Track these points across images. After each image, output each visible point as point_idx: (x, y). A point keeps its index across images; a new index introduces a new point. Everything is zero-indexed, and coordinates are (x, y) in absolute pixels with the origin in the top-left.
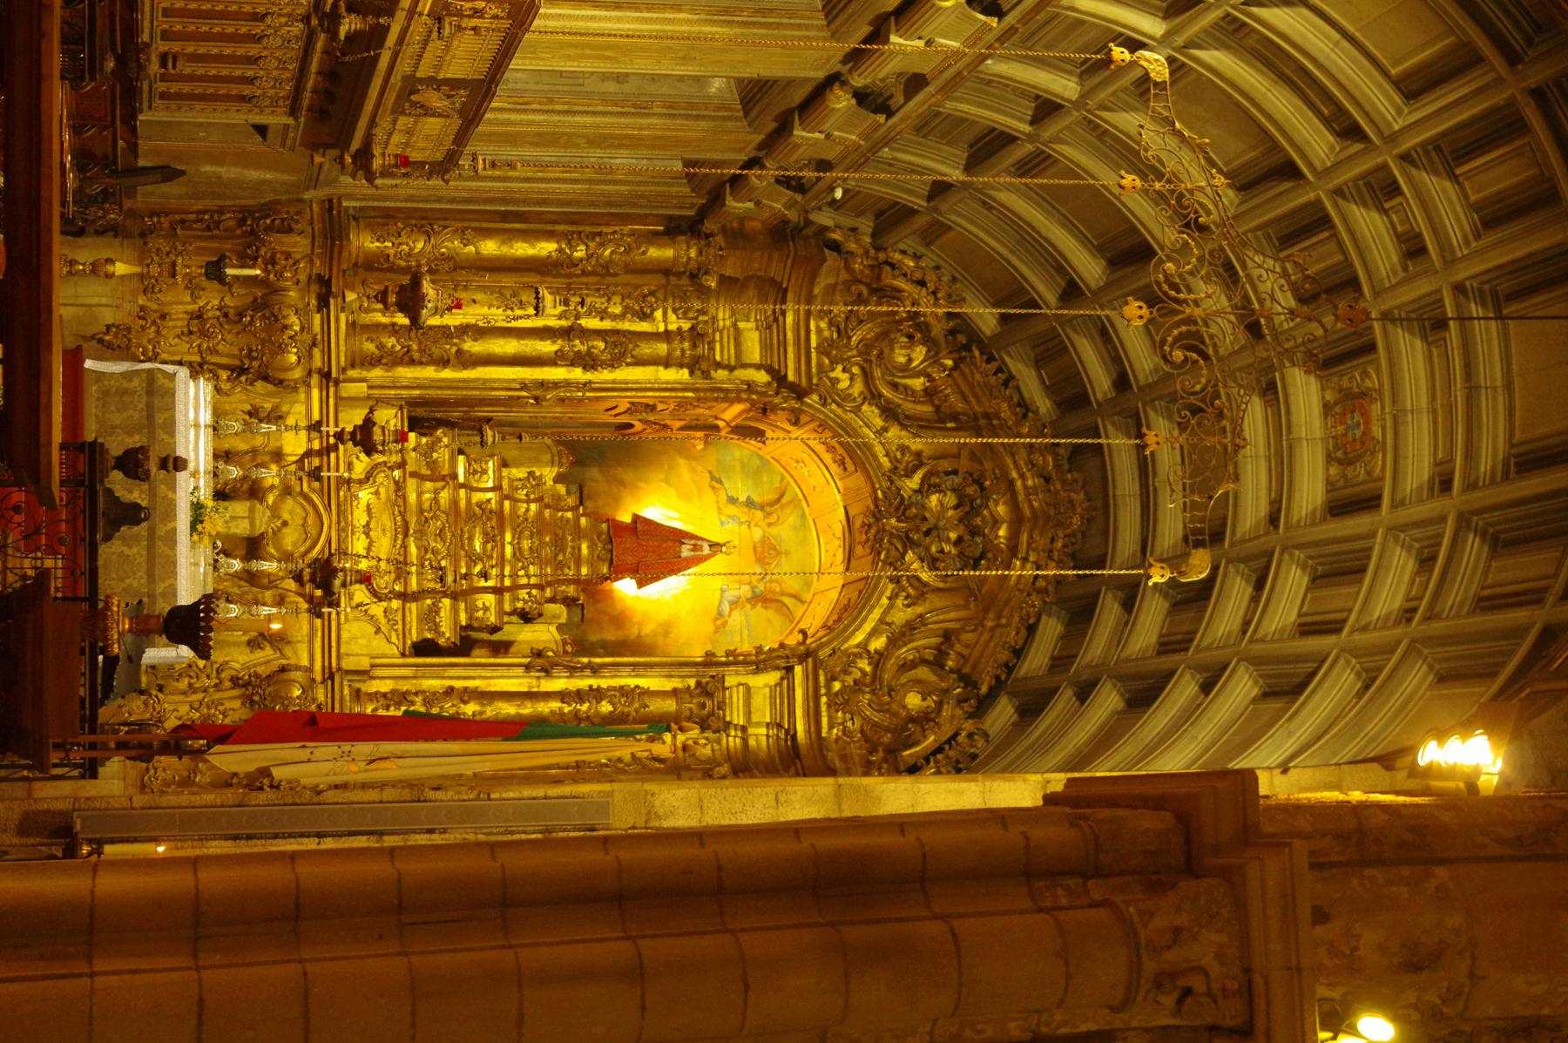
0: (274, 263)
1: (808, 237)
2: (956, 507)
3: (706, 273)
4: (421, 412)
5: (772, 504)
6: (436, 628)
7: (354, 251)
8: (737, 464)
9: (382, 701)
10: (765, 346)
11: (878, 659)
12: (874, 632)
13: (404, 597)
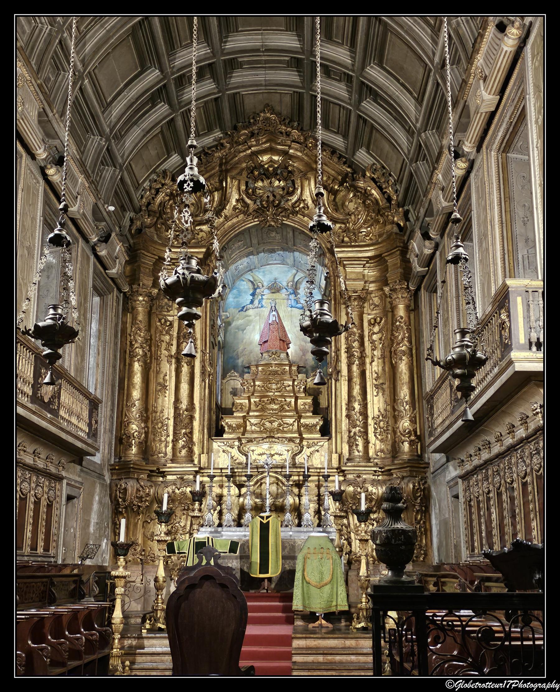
0: (142, 497)
1: (134, 243)
2: (263, 181)
3: (151, 293)
4: (213, 431)
5: (254, 285)
6: (315, 425)
7: (136, 459)
8: (236, 300)
9: (354, 447)
13: (302, 439)
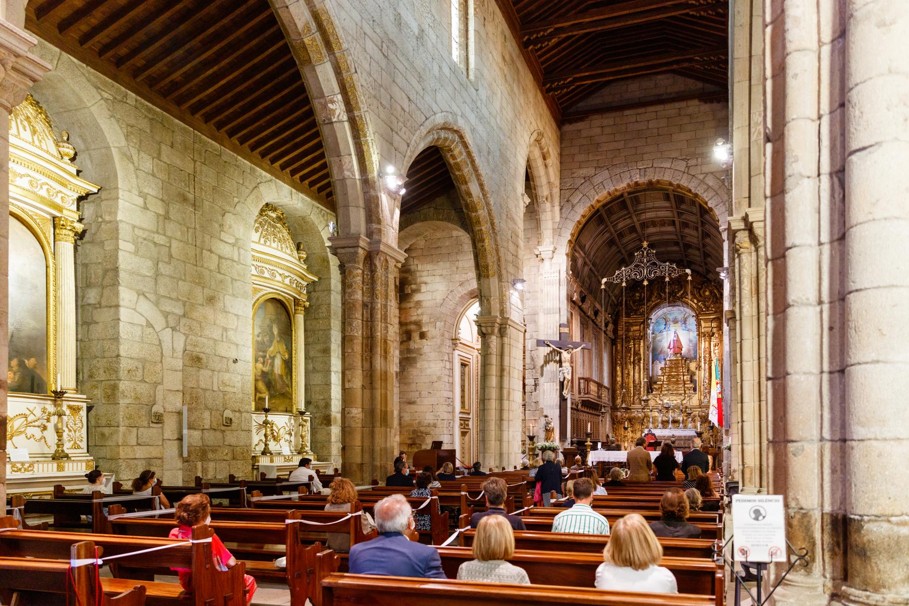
10: (636, 325)
11: (698, 301)
12: (693, 302)
